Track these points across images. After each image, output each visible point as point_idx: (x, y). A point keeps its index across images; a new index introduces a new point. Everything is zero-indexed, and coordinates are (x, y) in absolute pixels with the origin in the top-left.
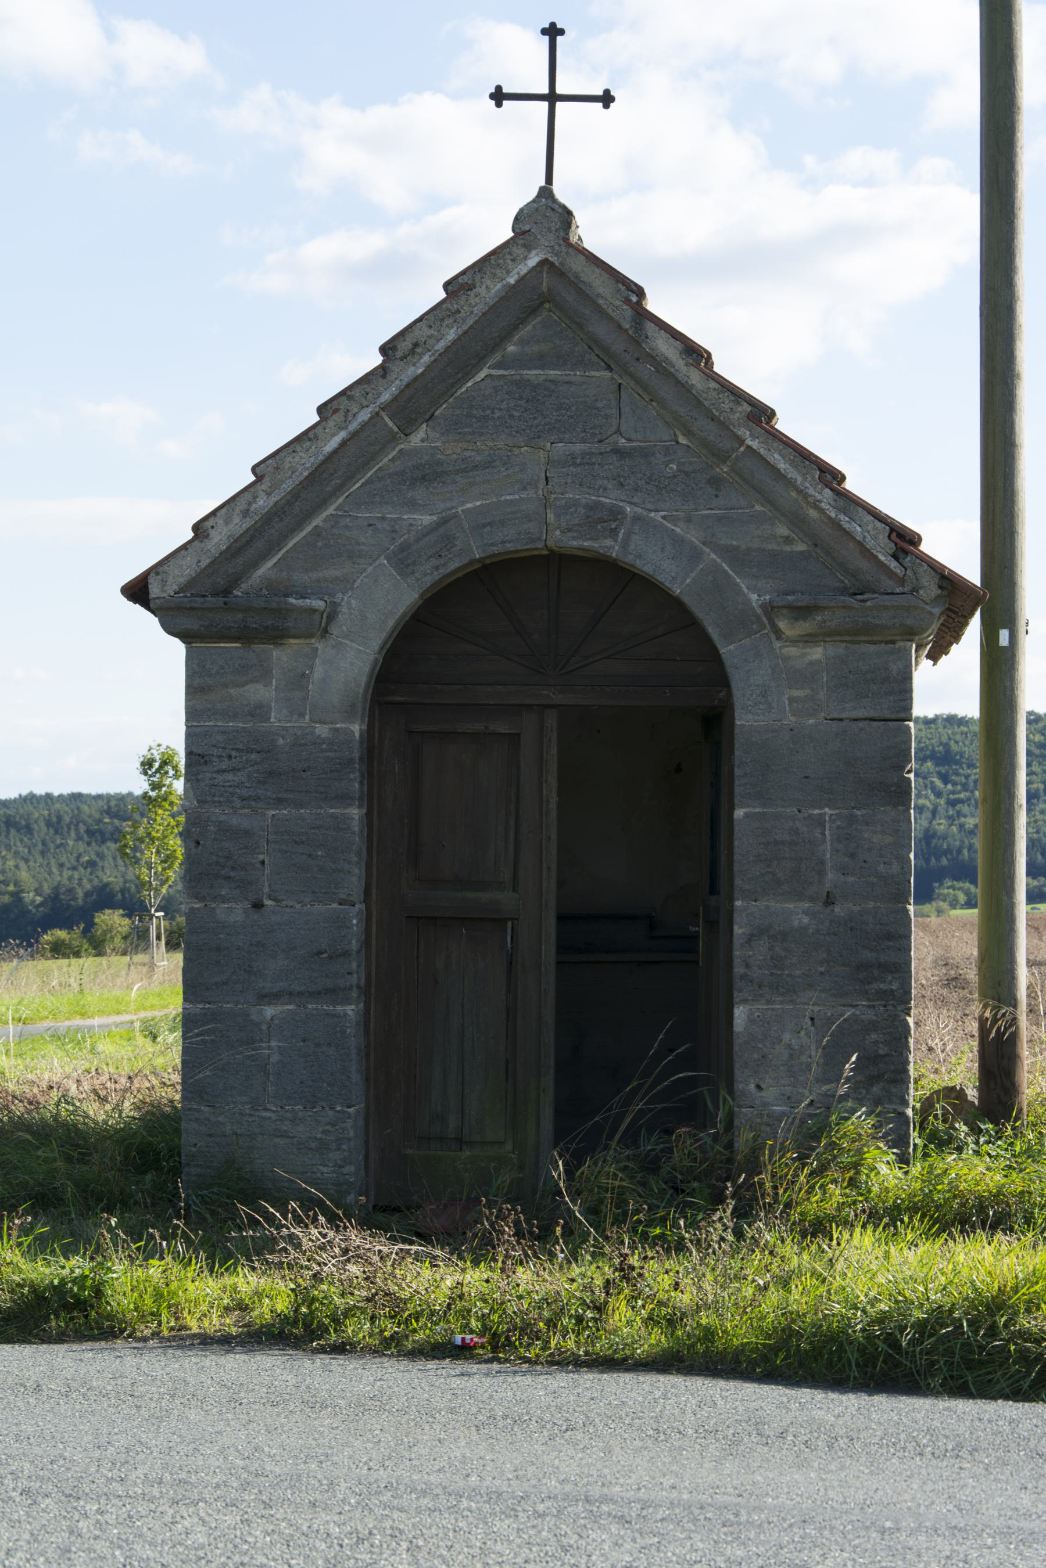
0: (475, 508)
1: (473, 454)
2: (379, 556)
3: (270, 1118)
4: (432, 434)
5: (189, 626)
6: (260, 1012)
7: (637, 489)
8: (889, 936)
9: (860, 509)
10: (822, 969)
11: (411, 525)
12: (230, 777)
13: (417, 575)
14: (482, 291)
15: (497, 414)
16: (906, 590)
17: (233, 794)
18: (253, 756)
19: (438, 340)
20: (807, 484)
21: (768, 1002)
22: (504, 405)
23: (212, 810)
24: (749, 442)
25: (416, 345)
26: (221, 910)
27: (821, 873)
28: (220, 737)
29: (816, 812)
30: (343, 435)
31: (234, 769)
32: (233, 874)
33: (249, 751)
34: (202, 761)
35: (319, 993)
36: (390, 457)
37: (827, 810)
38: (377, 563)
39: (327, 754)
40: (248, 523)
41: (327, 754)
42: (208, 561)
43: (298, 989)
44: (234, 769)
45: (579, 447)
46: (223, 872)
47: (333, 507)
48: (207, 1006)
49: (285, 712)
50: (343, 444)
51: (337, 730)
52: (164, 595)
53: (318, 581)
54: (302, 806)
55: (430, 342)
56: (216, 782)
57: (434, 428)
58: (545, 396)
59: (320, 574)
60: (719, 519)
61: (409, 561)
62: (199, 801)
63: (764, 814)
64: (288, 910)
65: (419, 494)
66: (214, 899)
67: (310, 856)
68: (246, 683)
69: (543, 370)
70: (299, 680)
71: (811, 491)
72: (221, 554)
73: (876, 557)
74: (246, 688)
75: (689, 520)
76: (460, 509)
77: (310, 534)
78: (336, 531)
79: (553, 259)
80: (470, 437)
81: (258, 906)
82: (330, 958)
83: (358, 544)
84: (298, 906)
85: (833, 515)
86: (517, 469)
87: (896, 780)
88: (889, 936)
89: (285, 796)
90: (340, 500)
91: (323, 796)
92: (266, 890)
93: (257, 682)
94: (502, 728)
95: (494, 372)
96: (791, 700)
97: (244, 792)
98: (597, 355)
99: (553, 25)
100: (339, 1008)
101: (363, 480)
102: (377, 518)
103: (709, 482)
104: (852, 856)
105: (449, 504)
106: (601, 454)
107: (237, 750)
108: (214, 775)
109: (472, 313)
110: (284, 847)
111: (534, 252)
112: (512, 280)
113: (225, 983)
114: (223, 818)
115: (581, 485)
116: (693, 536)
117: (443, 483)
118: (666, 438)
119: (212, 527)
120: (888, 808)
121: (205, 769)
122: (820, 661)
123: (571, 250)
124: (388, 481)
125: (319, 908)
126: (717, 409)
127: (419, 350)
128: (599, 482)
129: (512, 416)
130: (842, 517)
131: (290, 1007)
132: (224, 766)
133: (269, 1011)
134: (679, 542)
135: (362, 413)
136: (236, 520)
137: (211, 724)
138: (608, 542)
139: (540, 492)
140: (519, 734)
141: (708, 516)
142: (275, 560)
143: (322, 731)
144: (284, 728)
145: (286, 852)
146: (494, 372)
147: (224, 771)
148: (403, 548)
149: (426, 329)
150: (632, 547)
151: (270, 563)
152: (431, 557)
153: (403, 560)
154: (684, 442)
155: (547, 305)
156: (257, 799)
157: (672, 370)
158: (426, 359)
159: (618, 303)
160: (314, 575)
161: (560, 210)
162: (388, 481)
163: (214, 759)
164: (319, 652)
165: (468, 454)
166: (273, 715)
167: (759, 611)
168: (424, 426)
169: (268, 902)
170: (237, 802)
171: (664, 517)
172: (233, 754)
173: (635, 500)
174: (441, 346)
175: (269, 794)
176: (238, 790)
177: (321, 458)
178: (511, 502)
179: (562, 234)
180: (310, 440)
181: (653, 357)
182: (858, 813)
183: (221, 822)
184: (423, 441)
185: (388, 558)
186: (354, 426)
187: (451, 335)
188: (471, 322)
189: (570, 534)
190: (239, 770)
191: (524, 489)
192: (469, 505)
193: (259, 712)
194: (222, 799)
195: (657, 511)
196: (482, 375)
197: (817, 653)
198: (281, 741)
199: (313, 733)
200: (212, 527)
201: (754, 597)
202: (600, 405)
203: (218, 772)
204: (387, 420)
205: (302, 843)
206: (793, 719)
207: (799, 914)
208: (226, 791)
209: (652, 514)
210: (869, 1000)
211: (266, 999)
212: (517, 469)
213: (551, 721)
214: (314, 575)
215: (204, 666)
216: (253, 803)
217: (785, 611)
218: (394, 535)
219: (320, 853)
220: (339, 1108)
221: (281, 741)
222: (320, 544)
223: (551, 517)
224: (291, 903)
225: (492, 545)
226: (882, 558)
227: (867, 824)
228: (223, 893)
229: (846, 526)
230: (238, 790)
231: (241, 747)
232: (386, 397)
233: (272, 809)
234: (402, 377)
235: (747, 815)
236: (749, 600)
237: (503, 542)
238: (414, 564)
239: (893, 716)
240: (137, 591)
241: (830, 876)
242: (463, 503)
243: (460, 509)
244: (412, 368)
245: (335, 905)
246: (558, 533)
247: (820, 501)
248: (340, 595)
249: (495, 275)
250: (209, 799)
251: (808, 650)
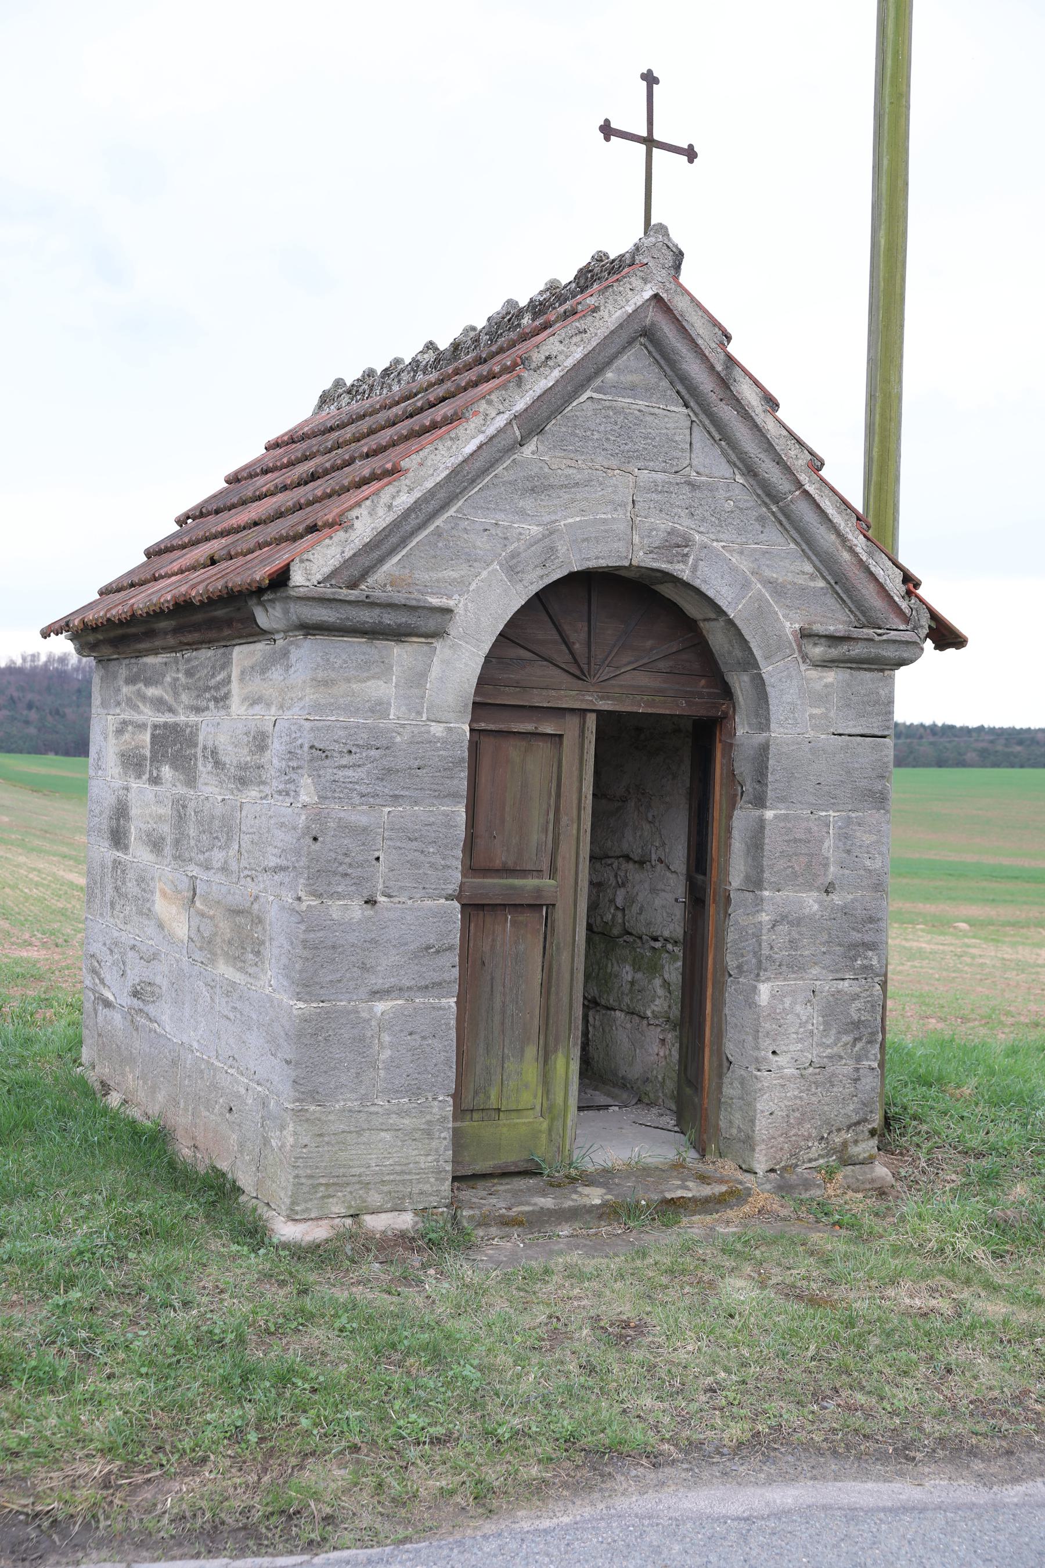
0: (575, 522)
1: (575, 471)
2: (492, 561)
3: (377, 1113)
4: (541, 448)
5: (326, 618)
6: (371, 1010)
7: (703, 519)
8: (871, 920)
9: (883, 556)
10: (824, 949)
11: (520, 534)
12: (350, 773)
13: (524, 582)
14: (606, 315)
15: (596, 436)
16: (909, 628)
17: (352, 790)
18: (373, 753)
19: (567, 357)
20: (848, 530)
21: (785, 980)
22: (602, 428)
23: (332, 806)
24: (807, 487)
25: (548, 358)
26: (335, 909)
27: (826, 866)
28: (341, 733)
29: (824, 814)
30: (481, 438)
31: (354, 765)
32: (349, 871)
33: (369, 747)
34: (324, 755)
35: (427, 987)
36: (505, 465)
37: (831, 813)
38: (490, 569)
39: (441, 752)
40: (389, 519)
41: (441, 752)
42: (351, 553)
43: (408, 985)
44: (354, 765)
45: (660, 477)
46: (340, 869)
47: (454, 509)
48: (321, 1004)
49: (403, 708)
50: (480, 447)
51: (450, 729)
52: (307, 584)
53: (438, 581)
54: (416, 803)
55: (561, 358)
56: (336, 777)
57: (543, 442)
58: (635, 424)
59: (440, 575)
60: (765, 553)
61: (519, 569)
62: (319, 797)
63: (787, 815)
64: (399, 906)
65: (527, 503)
66: (331, 896)
67: (422, 852)
68: (368, 679)
69: (635, 399)
70: (418, 678)
71: (850, 536)
72: (638, 567)
73: (891, 598)
74: (369, 683)
75: (741, 553)
76: (562, 523)
77: (432, 533)
78: (454, 532)
79: (664, 296)
80: (572, 455)
81: (371, 902)
82: (438, 952)
83: (475, 547)
84: (410, 902)
85: (864, 559)
86: (610, 490)
87: (880, 788)
88: (871, 920)
89: (402, 793)
90: (460, 503)
91: (437, 794)
92: (380, 887)
93: (378, 678)
94: (548, 728)
95: (595, 395)
96: (811, 716)
97: (363, 789)
98: (678, 392)
99: (650, 71)
100: (443, 1000)
101: (480, 486)
102: (492, 524)
103: (757, 520)
104: (848, 852)
105: (553, 518)
106: (677, 484)
107: (358, 746)
108: (335, 771)
109: (596, 334)
110: (398, 844)
111: (649, 285)
112: (630, 309)
113: (339, 981)
114: (342, 815)
115: (661, 511)
116: (744, 565)
117: (549, 496)
118: (727, 476)
119: (357, 518)
120: (874, 811)
121: (327, 763)
122: (832, 684)
123: (679, 289)
124: (503, 489)
125: (429, 903)
126: (786, 455)
127: (550, 363)
128: (675, 510)
129: (608, 439)
130: (871, 561)
131: (400, 1002)
132: (344, 761)
133: (381, 1007)
134: (733, 569)
135: (499, 418)
136: (381, 511)
137: (333, 718)
138: (681, 566)
139: (628, 514)
140: (561, 736)
141: (755, 550)
142: (399, 557)
143: (437, 730)
144: (403, 726)
145: (400, 848)
146: (595, 395)
147: (345, 767)
148: (514, 555)
149: (557, 344)
150: (699, 573)
151: (395, 559)
152: (536, 566)
153: (513, 569)
154: (741, 481)
155: (642, 340)
156: (375, 796)
157: (753, 414)
158: (556, 374)
159: (714, 345)
160: (435, 575)
161: (674, 249)
162: (503, 489)
163: (336, 754)
164: (438, 652)
165: (571, 471)
166: (392, 711)
167: (791, 637)
168: (535, 439)
169: (381, 899)
170: (357, 800)
171: (723, 547)
172: (354, 750)
173: (702, 529)
174: (569, 363)
175: (386, 791)
176: (357, 787)
177: (461, 459)
178: (604, 521)
179: (673, 272)
180: (451, 439)
181: (738, 400)
182: (853, 815)
183: (340, 819)
184: (533, 453)
185: (501, 565)
186: (491, 430)
187: (578, 354)
188: (595, 344)
189: (651, 555)
190: (359, 766)
191: (616, 510)
192: (570, 520)
193: (379, 708)
194: (341, 796)
195: (717, 541)
196: (584, 397)
197: (830, 676)
198: (398, 739)
199: (429, 732)
200: (357, 518)
201: (788, 624)
202: (677, 438)
203: (340, 767)
204: (516, 428)
205: (416, 839)
206: (812, 733)
207: (811, 902)
208: (346, 788)
209: (715, 544)
210: (855, 974)
211: (378, 995)
212: (610, 490)
213: (591, 720)
214: (435, 575)
215: (328, 660)
216: (371, 800)
217: (823, 640)
218: (506, 542)
219: (431, 850)
220: (441, 1099)
221: (398, 739)
222: (440, 545)
223: (636, 539)
224: (402, 899)
225: (588, 559)
226: (896, 599)
227: (859, 825)
228: (340, 890)
229: (873, 569)
230: (357, 787)
231: (361, 743)
232: (520, 405)
233: (389, 806)
234: (535, 388)
235: (776, 817)
236: (784, 627)
237: (597, 558)
238: (523, 571)
239: (880, 734)
240: (946, 637)
241: (832, 869)
242: (565, 519)
243: (562, 523)
244: (544, 381)
245: (443, 901)
246: (641, 553)
247: (856, 546)
248: (456, 596)
249: (616, 301)
250: (329, 794)
251: (825, 674)
